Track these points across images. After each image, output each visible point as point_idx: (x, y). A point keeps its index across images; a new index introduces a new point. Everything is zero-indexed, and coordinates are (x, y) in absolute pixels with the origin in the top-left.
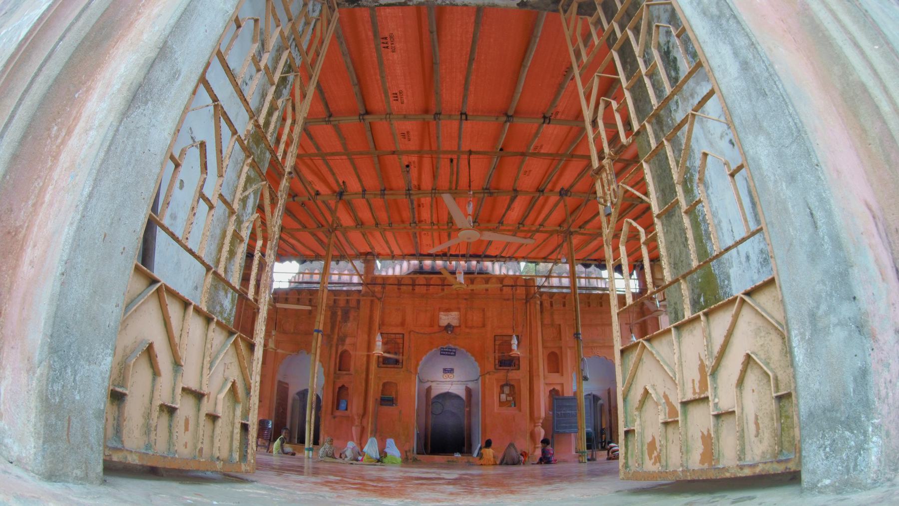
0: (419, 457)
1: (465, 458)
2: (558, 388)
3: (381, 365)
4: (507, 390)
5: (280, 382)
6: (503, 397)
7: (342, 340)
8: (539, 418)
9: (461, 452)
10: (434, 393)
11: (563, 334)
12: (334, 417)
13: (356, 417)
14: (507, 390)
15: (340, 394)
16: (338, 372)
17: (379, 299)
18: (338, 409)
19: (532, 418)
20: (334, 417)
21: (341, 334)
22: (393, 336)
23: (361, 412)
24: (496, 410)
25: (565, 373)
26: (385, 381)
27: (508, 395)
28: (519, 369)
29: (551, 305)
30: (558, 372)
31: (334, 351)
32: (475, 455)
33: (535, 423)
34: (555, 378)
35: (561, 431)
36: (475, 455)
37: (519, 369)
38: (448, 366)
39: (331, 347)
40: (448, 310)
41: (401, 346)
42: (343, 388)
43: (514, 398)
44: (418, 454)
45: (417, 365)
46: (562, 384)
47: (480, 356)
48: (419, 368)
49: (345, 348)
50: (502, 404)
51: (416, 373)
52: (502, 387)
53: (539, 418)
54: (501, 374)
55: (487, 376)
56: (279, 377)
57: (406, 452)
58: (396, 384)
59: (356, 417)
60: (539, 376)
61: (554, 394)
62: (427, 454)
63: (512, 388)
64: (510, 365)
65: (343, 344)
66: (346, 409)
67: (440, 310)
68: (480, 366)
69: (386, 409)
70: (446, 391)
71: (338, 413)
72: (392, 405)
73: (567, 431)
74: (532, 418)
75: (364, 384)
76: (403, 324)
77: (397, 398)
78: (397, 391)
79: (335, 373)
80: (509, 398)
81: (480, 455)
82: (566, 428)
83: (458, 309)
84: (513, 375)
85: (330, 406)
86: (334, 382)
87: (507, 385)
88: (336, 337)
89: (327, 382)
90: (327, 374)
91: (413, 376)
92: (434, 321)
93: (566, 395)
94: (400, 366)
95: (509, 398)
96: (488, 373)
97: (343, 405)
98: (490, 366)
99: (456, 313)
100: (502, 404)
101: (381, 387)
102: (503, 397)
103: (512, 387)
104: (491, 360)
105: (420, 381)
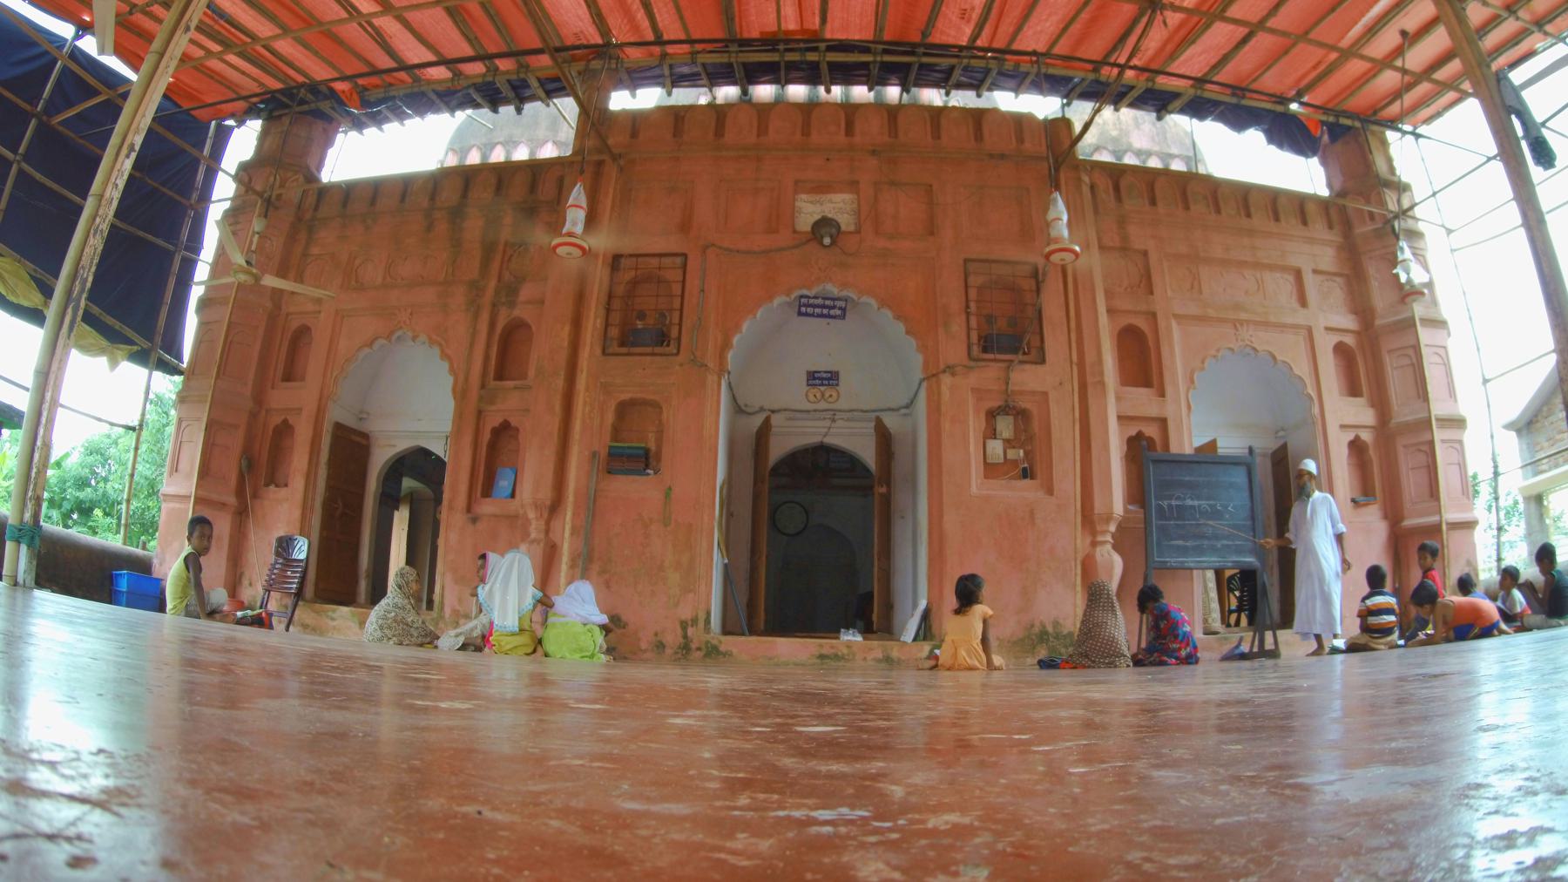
0: (730, 643)
1: (877, 647)
2: (1151, 431)
3: (615, 348)
4: (1005, 426)
5: (339, 427)
6: (996, 448)
7: (509, 292)
8: (1108, 518)
9: (868, 630)
10: (778, 449)
11: (1156, 279)
12: (474, 520)
13: (531, 515)
14: (1005, 426)
15: (495, 448)
16: (493, 384)
17: (615, 158)
18: (487, 491)
19: (1089, 520)
20: (474, 520)
21: (507, 276)
22: (654, 262)
23: (546, 494)
24: (974, 489)
25: (1169, 390)
26: (625, 396)
27: (1008, 443)
28: (1042, 361)
29: (1119, 199)
30: (1147, 383)
31: (483, 327)
32: (909, 634)
33: (1094, 533)
34: (1142, 401)
35: (1172, 560)
36: (909, 634)
37: (1042, 361)
38: (822, 365)
39: (476, 315)
40: (822, 188)
41: (677, 289)
42: (505, 430)
43: (1026, 453)
44: (726, 631)
45: (726, 345)
46: (1163, 422)
47: (922, 322)
48: (730, 355)
49: (517, 312)
50: (991, 470)
51: (722, 369)
52: (991, 415)
53: (1108, 518)
54: (989, 374)
55: (946, 380)
56: (338, 413)
57: (684, 625)
58: (656, 405)
59: (531, 515)
60: (1102, 384)
61: (1145, 453)
62: (753, 631)
63: (1018, 419)
64: (1015, 350)
65: (512, 304)
66: (513, 495)
67: (799, 186)
68: (923, 348)
69: (626, 486)
70: (814, 440)
71: (486, 507)
72: (642, 472)
73: (1190, 561)
74: (1089, 520)
75: (558, 408)
76: (685, 226)
77: (659, 447)
78: (660, 433)
79: (483, 386)
80: (1011, 454)
81: (926, 630)
82: (1184, 551)
83: (853, 186)
84: (1027, 378)
85: (463, 488)
86: (480, 412)
87: (1005, 410)
88: (493, 283)
89: (459, 416)
90: (460, 394)
91: (711, 379)
92: (779, 216)
93: (1174, 449)
94: (672, 349)
95: (1011, 454)
96: (950, 369)
97: (504, 484)
98: (954, 347)
99: (847, 197)
100: (991, 470)
101: (610, 418)
102: (996, 448)
103: (1022, 415)
104: (958, 326)
105: (738, 410)
